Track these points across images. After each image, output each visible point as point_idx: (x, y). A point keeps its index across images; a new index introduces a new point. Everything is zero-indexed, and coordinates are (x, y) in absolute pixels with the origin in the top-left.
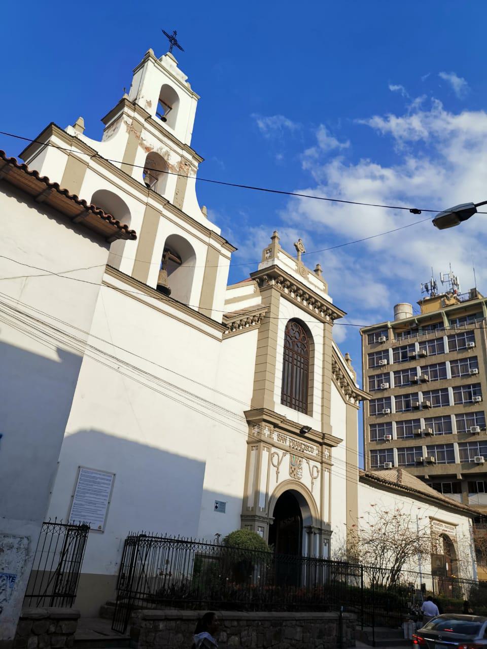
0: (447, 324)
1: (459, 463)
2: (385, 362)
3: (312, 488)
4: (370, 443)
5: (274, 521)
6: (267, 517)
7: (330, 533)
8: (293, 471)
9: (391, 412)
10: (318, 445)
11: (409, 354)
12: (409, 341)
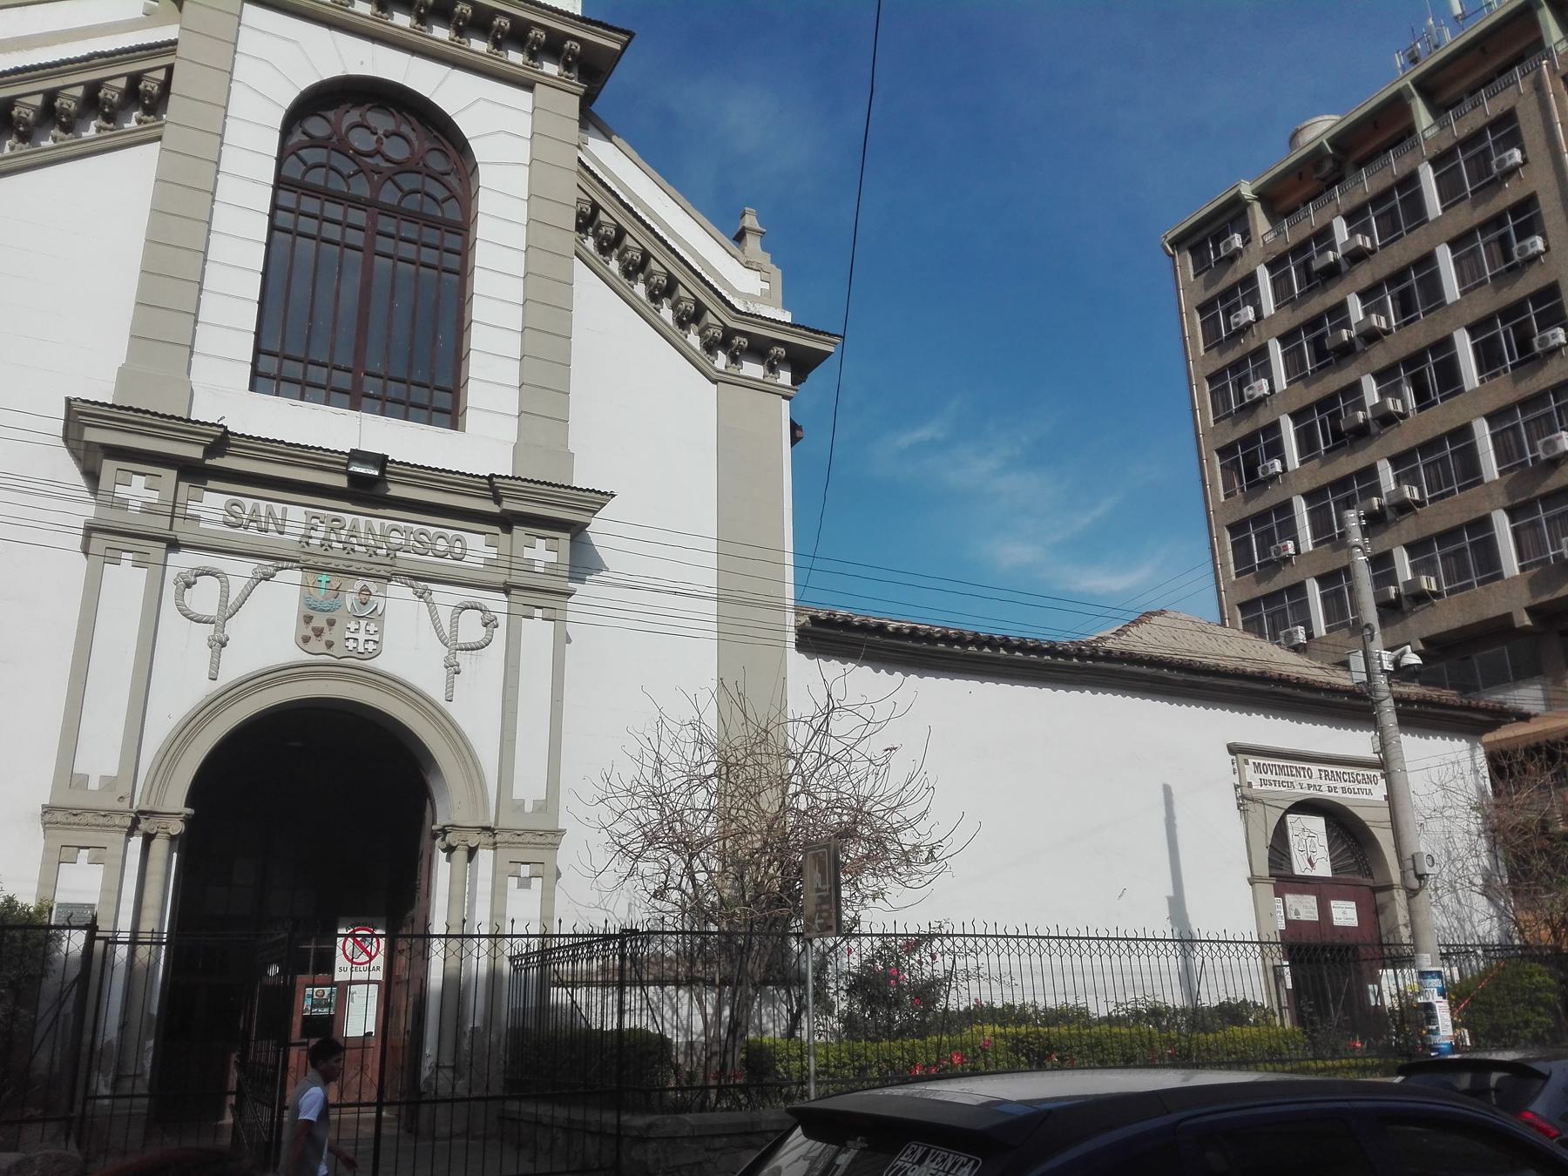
0: (1423, 117)
1: (1517, 572)
2: (1248, 313)
3: (450, 687)
4: (1234, 582)
5: (188, 821)
6: (125, 805)
7: (550, 839)
8: (319, 632)
9: (1285, 469)
10: (497, 530)
11: (1316, 265)
12: (1312, 219)
